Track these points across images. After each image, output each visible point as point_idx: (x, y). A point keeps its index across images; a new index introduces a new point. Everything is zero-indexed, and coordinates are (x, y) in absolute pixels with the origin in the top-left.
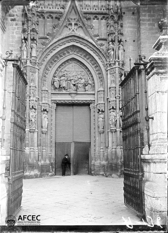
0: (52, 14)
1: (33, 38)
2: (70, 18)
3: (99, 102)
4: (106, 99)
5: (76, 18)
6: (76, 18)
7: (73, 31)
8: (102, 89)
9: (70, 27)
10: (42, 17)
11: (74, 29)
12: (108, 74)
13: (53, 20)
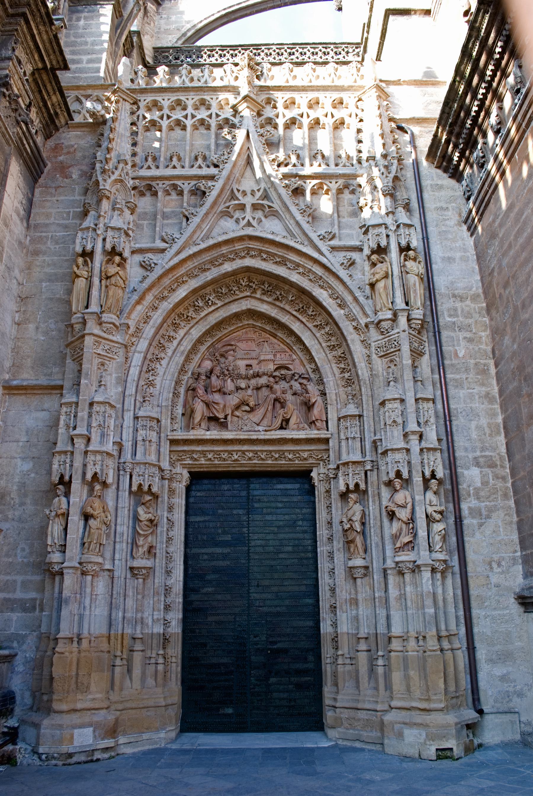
0: (179, 183)
1: (113, 248)
2: (238, 191)
3: (345, 458)
4: (368, 446)
5: (258, 190)
6: (258, 190)
7: (249, 224)
8: (352, 410)
9: (238, 214)
10: (148, 194)
11: (251, 221)
12: (374, 356)
13: (183, 200)
